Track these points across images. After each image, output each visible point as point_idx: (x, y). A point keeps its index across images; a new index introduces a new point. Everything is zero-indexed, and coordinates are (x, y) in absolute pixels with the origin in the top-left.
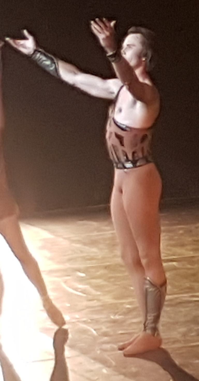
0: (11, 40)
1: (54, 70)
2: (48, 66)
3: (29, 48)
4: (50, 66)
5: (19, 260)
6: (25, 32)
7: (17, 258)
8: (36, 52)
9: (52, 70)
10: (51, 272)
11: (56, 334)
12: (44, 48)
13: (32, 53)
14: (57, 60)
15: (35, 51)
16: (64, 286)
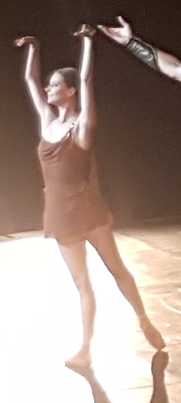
0: (103, 27)
1: (153, 61)
2: (145, 56)
3: (124, 37)
4: (148, 57)
5: (113, 275)
6: (120, 19)
7: (111, 272)
8: (132, 41)
9: (150, 62)
10: (148, 288)
11: (155, 358)
12: (141, 37)
13: (128, 42)
14: (156, 51)
15: (131, 40)
16: (164, 303)
